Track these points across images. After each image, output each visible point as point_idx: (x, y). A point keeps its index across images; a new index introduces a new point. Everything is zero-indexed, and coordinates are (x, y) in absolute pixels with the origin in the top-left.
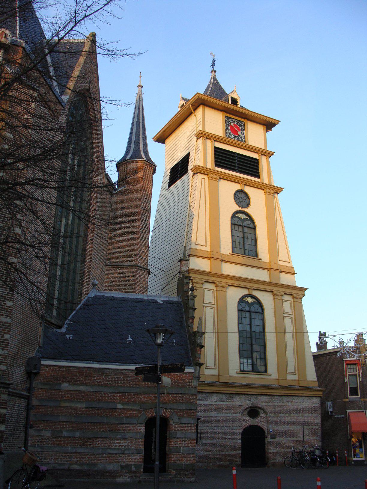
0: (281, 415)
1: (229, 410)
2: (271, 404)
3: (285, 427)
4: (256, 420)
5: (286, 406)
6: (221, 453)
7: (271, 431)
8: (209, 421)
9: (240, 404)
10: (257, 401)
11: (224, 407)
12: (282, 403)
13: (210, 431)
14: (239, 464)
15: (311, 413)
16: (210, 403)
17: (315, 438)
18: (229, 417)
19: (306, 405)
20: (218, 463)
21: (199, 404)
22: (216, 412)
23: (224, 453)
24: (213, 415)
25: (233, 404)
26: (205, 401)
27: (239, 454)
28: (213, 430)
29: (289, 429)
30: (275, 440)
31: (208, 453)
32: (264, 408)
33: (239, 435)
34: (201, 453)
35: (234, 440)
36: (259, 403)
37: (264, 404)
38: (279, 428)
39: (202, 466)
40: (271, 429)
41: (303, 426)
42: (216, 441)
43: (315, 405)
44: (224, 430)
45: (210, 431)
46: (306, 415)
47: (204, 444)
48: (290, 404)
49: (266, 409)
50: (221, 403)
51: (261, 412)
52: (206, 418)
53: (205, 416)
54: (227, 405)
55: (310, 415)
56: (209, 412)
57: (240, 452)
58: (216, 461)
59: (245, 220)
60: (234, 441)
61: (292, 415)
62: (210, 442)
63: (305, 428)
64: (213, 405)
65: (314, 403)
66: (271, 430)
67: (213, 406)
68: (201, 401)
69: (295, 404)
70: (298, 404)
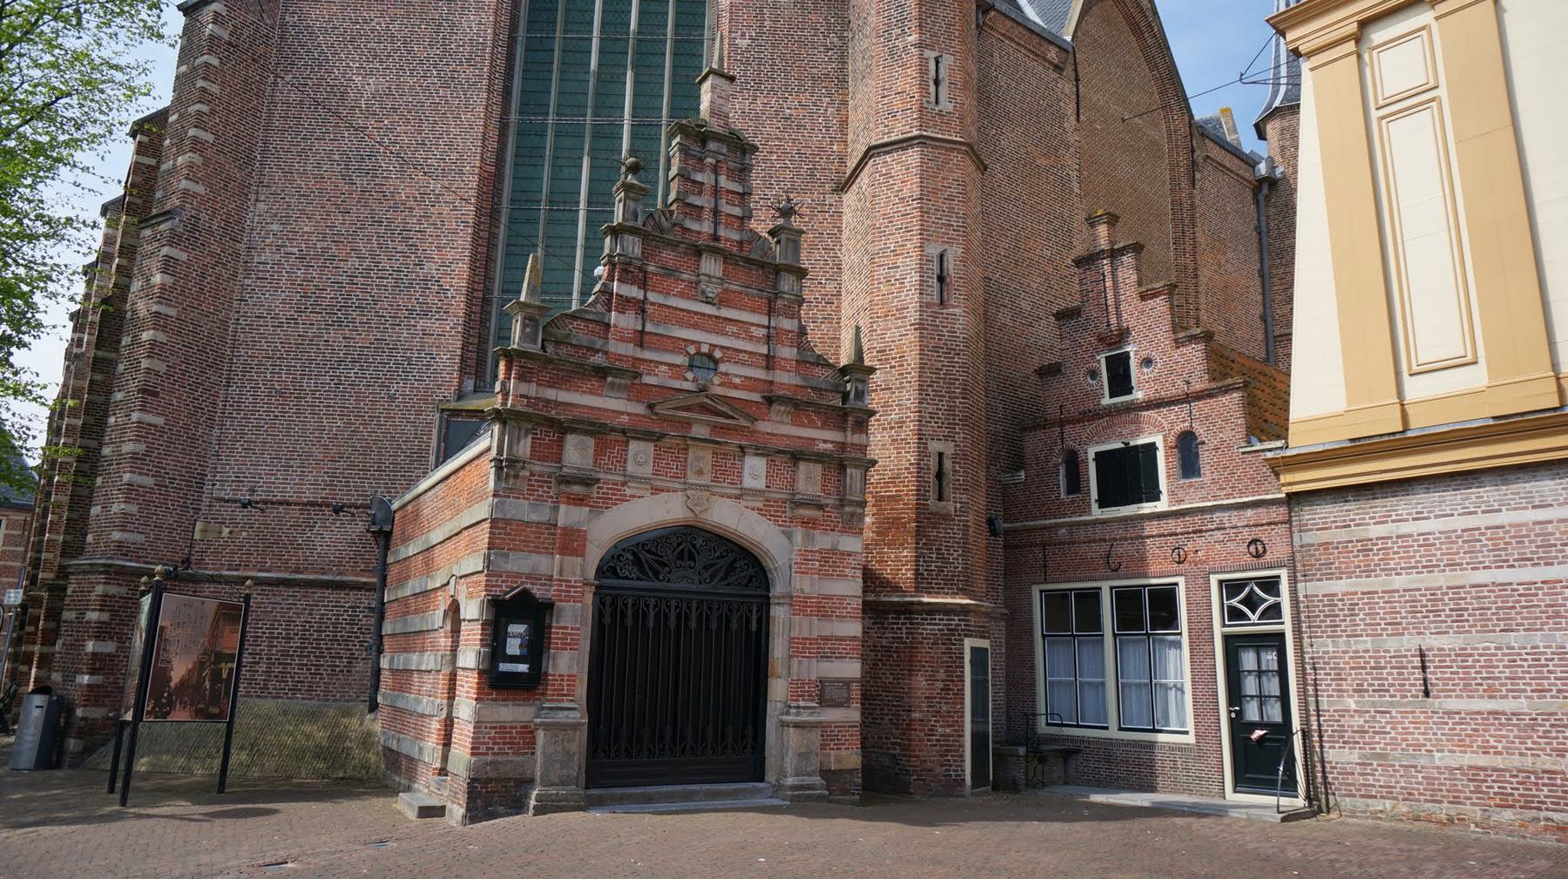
8: (1467, 609)
11: (1553, 534)
16: (1459, 523)
21: (1398, 537)
22: (1501, 563)
31: (1482, 761)
34: (1437, 755)
39: (1451, 820)
42: (1523, 700)
47: (1449, 713)
50: (1531, 515)
53: (1438, 584)
64: (1479, 529)
68: (1407, 520)
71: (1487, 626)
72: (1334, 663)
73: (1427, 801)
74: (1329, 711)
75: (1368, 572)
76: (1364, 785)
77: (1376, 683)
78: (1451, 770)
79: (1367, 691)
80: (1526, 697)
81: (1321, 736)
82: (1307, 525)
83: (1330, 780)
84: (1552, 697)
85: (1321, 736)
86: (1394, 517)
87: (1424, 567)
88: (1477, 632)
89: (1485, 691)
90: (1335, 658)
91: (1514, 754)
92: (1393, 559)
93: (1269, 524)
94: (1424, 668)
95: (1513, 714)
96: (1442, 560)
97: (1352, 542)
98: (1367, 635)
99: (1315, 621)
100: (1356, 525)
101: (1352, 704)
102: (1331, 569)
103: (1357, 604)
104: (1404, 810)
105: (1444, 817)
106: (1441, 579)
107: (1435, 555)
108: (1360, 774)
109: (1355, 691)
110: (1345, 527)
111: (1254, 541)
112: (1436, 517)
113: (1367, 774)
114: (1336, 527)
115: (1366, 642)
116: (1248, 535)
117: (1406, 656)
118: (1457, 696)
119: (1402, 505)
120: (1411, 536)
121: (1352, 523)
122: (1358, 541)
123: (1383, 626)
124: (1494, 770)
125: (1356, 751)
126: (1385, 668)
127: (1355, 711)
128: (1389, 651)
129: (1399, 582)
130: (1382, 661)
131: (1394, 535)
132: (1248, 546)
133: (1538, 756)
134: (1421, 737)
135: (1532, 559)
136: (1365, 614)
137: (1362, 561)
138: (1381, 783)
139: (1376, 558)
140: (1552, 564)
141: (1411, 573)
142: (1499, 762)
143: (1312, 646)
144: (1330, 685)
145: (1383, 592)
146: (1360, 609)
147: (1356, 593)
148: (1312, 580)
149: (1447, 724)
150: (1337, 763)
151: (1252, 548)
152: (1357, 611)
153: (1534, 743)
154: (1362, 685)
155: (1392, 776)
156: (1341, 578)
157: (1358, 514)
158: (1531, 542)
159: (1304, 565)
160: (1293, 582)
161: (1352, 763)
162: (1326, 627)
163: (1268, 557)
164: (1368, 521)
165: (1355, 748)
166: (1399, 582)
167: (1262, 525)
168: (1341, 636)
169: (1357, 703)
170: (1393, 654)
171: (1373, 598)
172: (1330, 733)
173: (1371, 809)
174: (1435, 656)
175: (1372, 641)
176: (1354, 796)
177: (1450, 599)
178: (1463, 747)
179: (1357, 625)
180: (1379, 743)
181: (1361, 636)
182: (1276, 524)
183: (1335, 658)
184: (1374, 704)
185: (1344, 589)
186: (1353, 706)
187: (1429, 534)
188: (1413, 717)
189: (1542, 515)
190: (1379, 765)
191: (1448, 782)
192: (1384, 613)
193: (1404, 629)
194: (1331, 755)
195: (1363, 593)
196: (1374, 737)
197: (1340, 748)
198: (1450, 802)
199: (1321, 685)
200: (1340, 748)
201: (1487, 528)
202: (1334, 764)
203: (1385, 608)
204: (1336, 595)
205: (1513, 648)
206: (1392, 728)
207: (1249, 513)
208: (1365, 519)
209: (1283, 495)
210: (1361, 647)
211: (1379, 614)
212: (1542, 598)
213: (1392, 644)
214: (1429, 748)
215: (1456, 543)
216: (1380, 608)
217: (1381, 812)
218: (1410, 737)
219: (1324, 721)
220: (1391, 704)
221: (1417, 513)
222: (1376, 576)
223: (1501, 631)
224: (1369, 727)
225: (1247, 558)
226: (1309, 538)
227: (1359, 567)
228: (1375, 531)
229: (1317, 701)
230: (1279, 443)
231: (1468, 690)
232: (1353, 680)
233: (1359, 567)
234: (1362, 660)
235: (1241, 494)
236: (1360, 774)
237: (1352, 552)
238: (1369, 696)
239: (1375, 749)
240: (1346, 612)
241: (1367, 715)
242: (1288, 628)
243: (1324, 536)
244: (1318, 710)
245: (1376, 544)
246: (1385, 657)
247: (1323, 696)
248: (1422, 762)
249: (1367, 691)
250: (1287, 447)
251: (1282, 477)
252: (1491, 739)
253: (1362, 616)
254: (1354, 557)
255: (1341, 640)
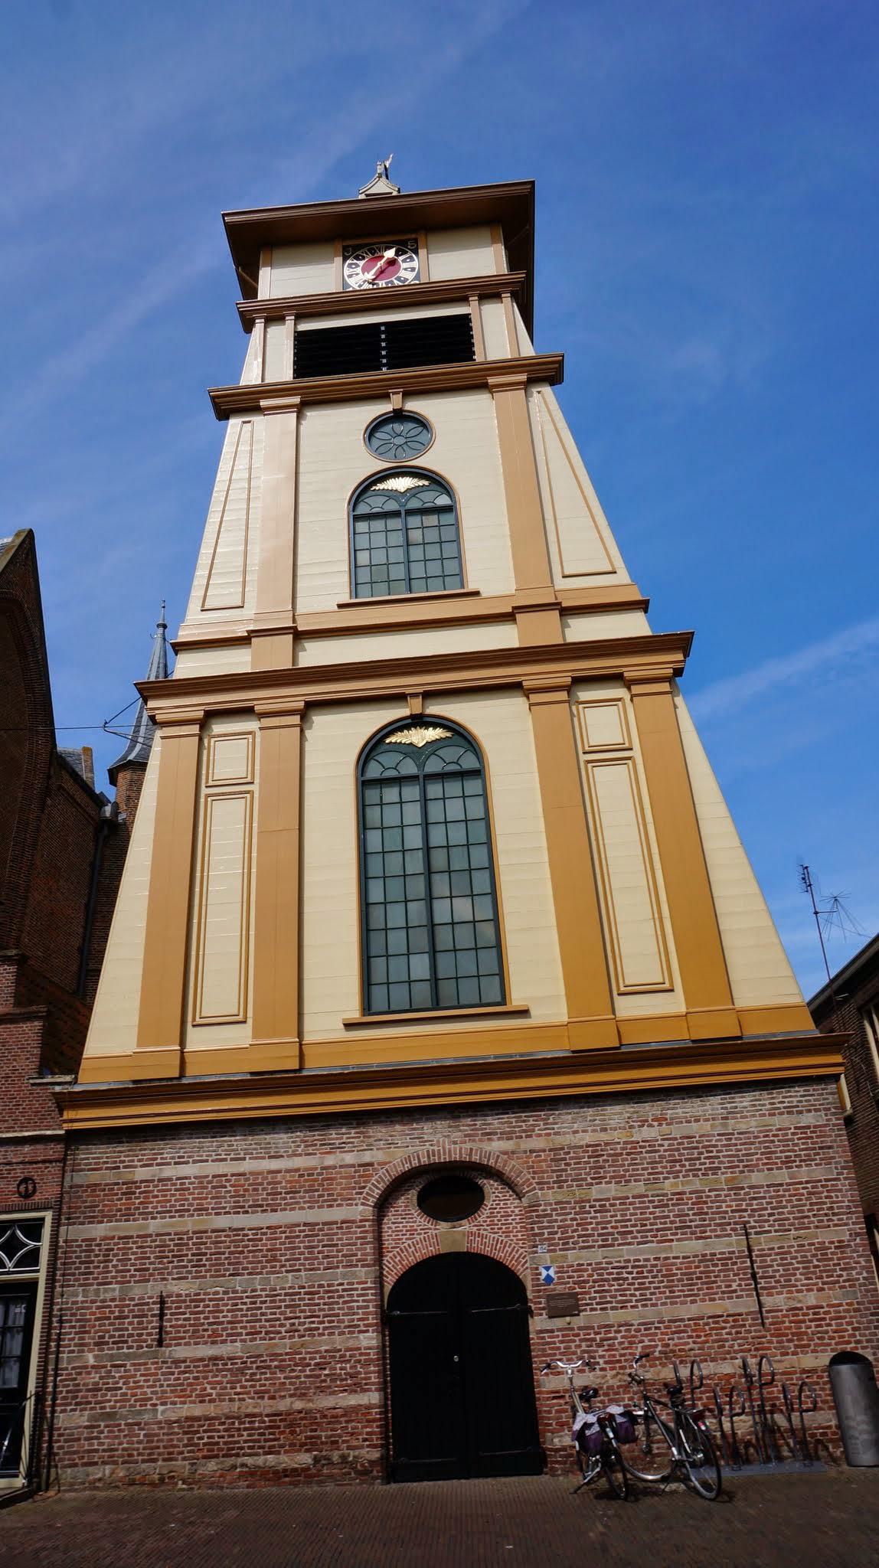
0: (595, 1192)
1: (306, 1192)
2: (536, 1143)
3: (627, 1252)
4: (465, 1226)
5: (625, 1143)
6: (266, 1406)
7: (549, 1279)
9: (367, 1157)
10: (457, 1136)
11: (280, 1183)
12: (605, 1130)
13: (210, 1300)
14: (371, 1462)
15: (787, 1163)
16: (212, 1169)
17: (834, 1296)
18: (305, 1224)
19: (752, 1124)
20: (249, 1461)
21: (160, 1180)
22: (239, 1209)
23: (283, 1405)
24: (223, 1221)
25: (330, 1160)
26: (187, 1163)
27: (369, 1407)
28: (225, 1293)
29: (656, 1259)
30: (578, 1321)
31: (198, 1410)
32: (499, 1166)
33: (366, 1306)
34: (160, 1408)
35: (336, 1337)
36: (468, 1146)
37: (497, 1145)
38: (597, 1255)
39: (162, 1480)
40: (547, 1269)
41: (747, 1234)
42: (238, 1344)
43: (808, 1119)
44: (284, 1289)
45: (210, 1300)
46: (756, 1178)
47: (177, 1362)
48: (647, 1133)
49: (509, 1168)
51: (491, 1187)
52: (192, 1238)
54: (297, 1170)
55: (783, 1176)
56: (207, 1209)
57: (374, 1398)
58: (242, 1448)
59: (412, 492)
60: (339, 1341)
61: (669, 1186)
62: (206, 1351)
63: (761, 1243)
64: (226, 1175)
65: (800, 1112)
66: (544, 1273)
67: (228, 1181)
68: (169, 1164)
69: (677, 1131)
70: (694, 1128)
71: (219, 1270)
72: (81, 1314)
73: (144, 1461)
74: (66, 1369)
75: (128, 1215)
76: (89, 1451)
77: (117, 1334)
78: (169, 1423)
79: (107, 1343)
80: (241, 1341)
81: (54, 1399)
82: (79, 1164)
83: (55, 1451)
84: (261, 1339)
85: (54, 1399)
86: (159, 1161)
87: (177, 1211)
88: (211, 1276)
89: (209, 1336)
90: (83, 1308)
91: (224, 1400)
92: (152, 1203)
93: (44, 1162)
94: (162, 1315)
95: (230, 1359)
96: (191, 1205)
97: (118, 1184)
98: (117, 1283)
99: (70, 1269)
100: (125, 1167)
101: (91, 1359)
102: (94, 1212)
103: (112, 1250)
104: (121, 1474)
105: (156, 1477)
106: (189, 1224)
107: (187, 1200)
108: (86, 1439)
109: (96, 1344)
110: (114, 1168)
111: (25, 1180)
112: (194, 1162)
113: (92, 1438)
114: (107, 1169)
115: (114, 1290)
116: (20, 1172)
117: (147, 1304)
118: (186, 1344)
119: (168, 1150)
120: (170, 1179)
121: (121, 1165)
122: (123, 1184)
123: (132, 1272)
124: (207, 1418)
125: (87, 1412)
126: (128, 1317)
127: (93, 1367)
128: (132, 1299)
129: (154, 1226)
130: (126, 1309)
131: (156, 1179)
132: (19, 1185)
133: (244, 1400)
134: (149, 1391)
135: (261, 1206)
136: (118, 1260)
137: (124, 1204)
138: (105, 1447)
139: (137, 1201)
140: (276, 1211)
141: (165, 1218)
142: (211, 1410)
143: (62, 1295)
144: (73, 1339)
145: (138, 1237)
146: (115, 1255)
147: (113, 1238)
148: (74, 1224)
149: (173, 1373)
150: (65, 1429)
151: (22, 1188)
152: (111, 1258)
153: (242, 1387)
154: (103, 1337)
155: (117, 1437)
156: (102, 1222)
157: (128, 1156)
158: (264, 1189)
159: (70, 1208)
160: (57, 1224)
161: (80, 1427)
162: (80, 1274)
163: (37, 1198)
164: (136, 1163)
165: (85, 1409)
166: (154, 1226)
167: (37, 1162)
168: (92, 1285)
169: (96, 1357)
170: (137, 1302)
171: (128, 1243)
172: (64, 1394)
173: (91, 1478)
174: (173, 1302)
175: (121, 1289)
176: (76, 1465)
177: (194, 1244)
178: (184, 1396)
179: (108, 1272)
180: (110, 1401)
181: (111, 1283)
182: (51, 1162)
183: (83, 1308)
184: (112, 1357)
185: (103, 1234)
186: (91, 1361)
187: (186, 1178)
188: (146, 1369)
189: (275, 1165)
190: (106, 1426)
191: (165, 1437)
192: (136, 1259)
193: (151, 1275)
194: (62, 1420)
195: (119, 1238)
196: (106, 1395)
197: (72, 1410)
198: (165, 1460)
199: (64, 1340)
200: (72, 1410)
201: (233, 1175)
202: (62, 1431)
203: (136, 1253)
204: (94, 1240)
205: (237, 1292)
206: (124, 1384)
207: (27, 1149)
208: (133, 1161)
209: (62, 1132)
210: (109, 1296)
211: (130, 1259)
212: (265, 1244)
213: (137, 1291)
214: (154, 1401)
215: (207, 1188)
216: (133, 1254)
217: (100, 1480)
218: (139, 1391)
219: (61, 1381)
220: (128, 1356)
221: (179, 1157)
222: (134, 1220)
223: (230, 1275)
224: (104, 1384)
225: (15, 1199)
226: (79, 1178)
227: (120, 1210)
228: (141, 1174)
229: (57, 1358)
230: (68, 1078)
231: (196, 1337)
232: (96, 1332)
233: (120, 1210)
234: (108, 1310)
235: (23, 1128)
236: (86, 1439)
237: (117, 1194)
238: (109, 1349)
239: (104, 1408)
240: (101, 1258)
241: (103, 1370)
242: (42, 1277)
243: (94, 1177)
244: (56, 1369)
245: (140, 1187)
246: (129, 1305)
247: (64, 1352)
248: (146, 1417)
249: (107, 1343)
250: (76, 1083)
251: (65, 1113)
252: (208, 1387)
253: (114, 1263)
254: (118, 1200)
255: (92, 1288)
